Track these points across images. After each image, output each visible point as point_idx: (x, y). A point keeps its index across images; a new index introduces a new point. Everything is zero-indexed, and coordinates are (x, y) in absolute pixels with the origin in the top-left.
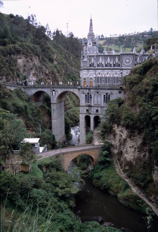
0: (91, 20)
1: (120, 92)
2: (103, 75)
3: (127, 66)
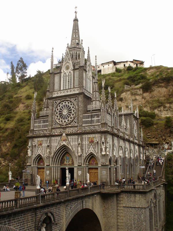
0: (76, 20)
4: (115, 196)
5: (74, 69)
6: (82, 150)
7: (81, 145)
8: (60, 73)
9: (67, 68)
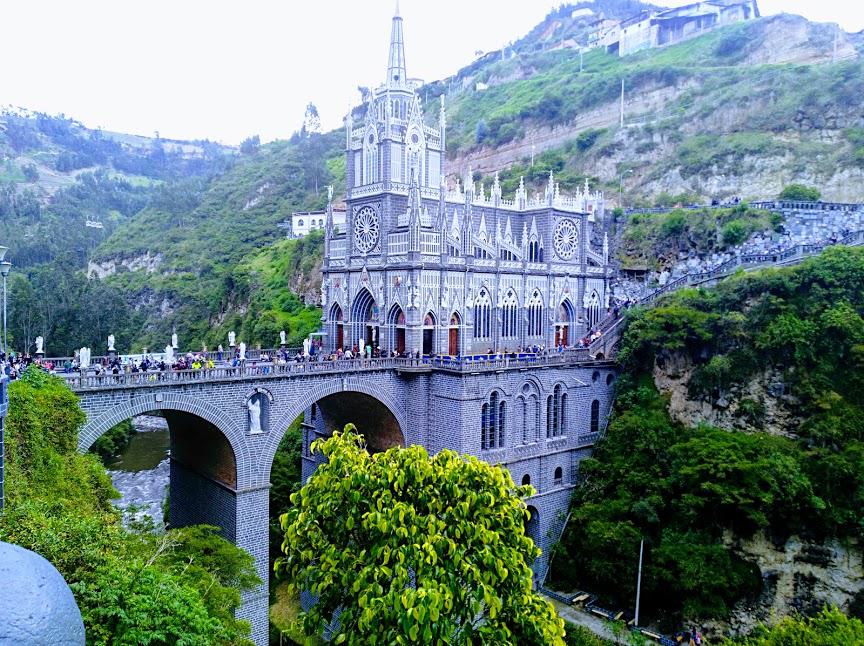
1: (595, 376)
2: (500, 299)
3: (565, 262)
4: (422, 379)
5: (379, 144)
6: (386, 298)
7: (384, 289)
8: (361, 150)
9: (371, 139)
